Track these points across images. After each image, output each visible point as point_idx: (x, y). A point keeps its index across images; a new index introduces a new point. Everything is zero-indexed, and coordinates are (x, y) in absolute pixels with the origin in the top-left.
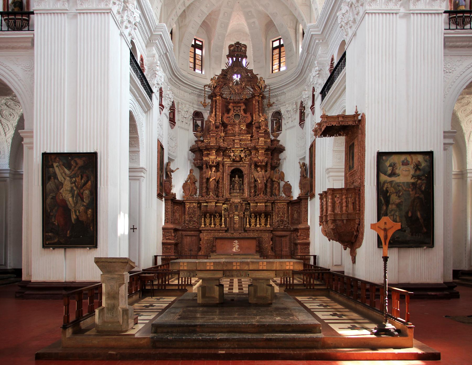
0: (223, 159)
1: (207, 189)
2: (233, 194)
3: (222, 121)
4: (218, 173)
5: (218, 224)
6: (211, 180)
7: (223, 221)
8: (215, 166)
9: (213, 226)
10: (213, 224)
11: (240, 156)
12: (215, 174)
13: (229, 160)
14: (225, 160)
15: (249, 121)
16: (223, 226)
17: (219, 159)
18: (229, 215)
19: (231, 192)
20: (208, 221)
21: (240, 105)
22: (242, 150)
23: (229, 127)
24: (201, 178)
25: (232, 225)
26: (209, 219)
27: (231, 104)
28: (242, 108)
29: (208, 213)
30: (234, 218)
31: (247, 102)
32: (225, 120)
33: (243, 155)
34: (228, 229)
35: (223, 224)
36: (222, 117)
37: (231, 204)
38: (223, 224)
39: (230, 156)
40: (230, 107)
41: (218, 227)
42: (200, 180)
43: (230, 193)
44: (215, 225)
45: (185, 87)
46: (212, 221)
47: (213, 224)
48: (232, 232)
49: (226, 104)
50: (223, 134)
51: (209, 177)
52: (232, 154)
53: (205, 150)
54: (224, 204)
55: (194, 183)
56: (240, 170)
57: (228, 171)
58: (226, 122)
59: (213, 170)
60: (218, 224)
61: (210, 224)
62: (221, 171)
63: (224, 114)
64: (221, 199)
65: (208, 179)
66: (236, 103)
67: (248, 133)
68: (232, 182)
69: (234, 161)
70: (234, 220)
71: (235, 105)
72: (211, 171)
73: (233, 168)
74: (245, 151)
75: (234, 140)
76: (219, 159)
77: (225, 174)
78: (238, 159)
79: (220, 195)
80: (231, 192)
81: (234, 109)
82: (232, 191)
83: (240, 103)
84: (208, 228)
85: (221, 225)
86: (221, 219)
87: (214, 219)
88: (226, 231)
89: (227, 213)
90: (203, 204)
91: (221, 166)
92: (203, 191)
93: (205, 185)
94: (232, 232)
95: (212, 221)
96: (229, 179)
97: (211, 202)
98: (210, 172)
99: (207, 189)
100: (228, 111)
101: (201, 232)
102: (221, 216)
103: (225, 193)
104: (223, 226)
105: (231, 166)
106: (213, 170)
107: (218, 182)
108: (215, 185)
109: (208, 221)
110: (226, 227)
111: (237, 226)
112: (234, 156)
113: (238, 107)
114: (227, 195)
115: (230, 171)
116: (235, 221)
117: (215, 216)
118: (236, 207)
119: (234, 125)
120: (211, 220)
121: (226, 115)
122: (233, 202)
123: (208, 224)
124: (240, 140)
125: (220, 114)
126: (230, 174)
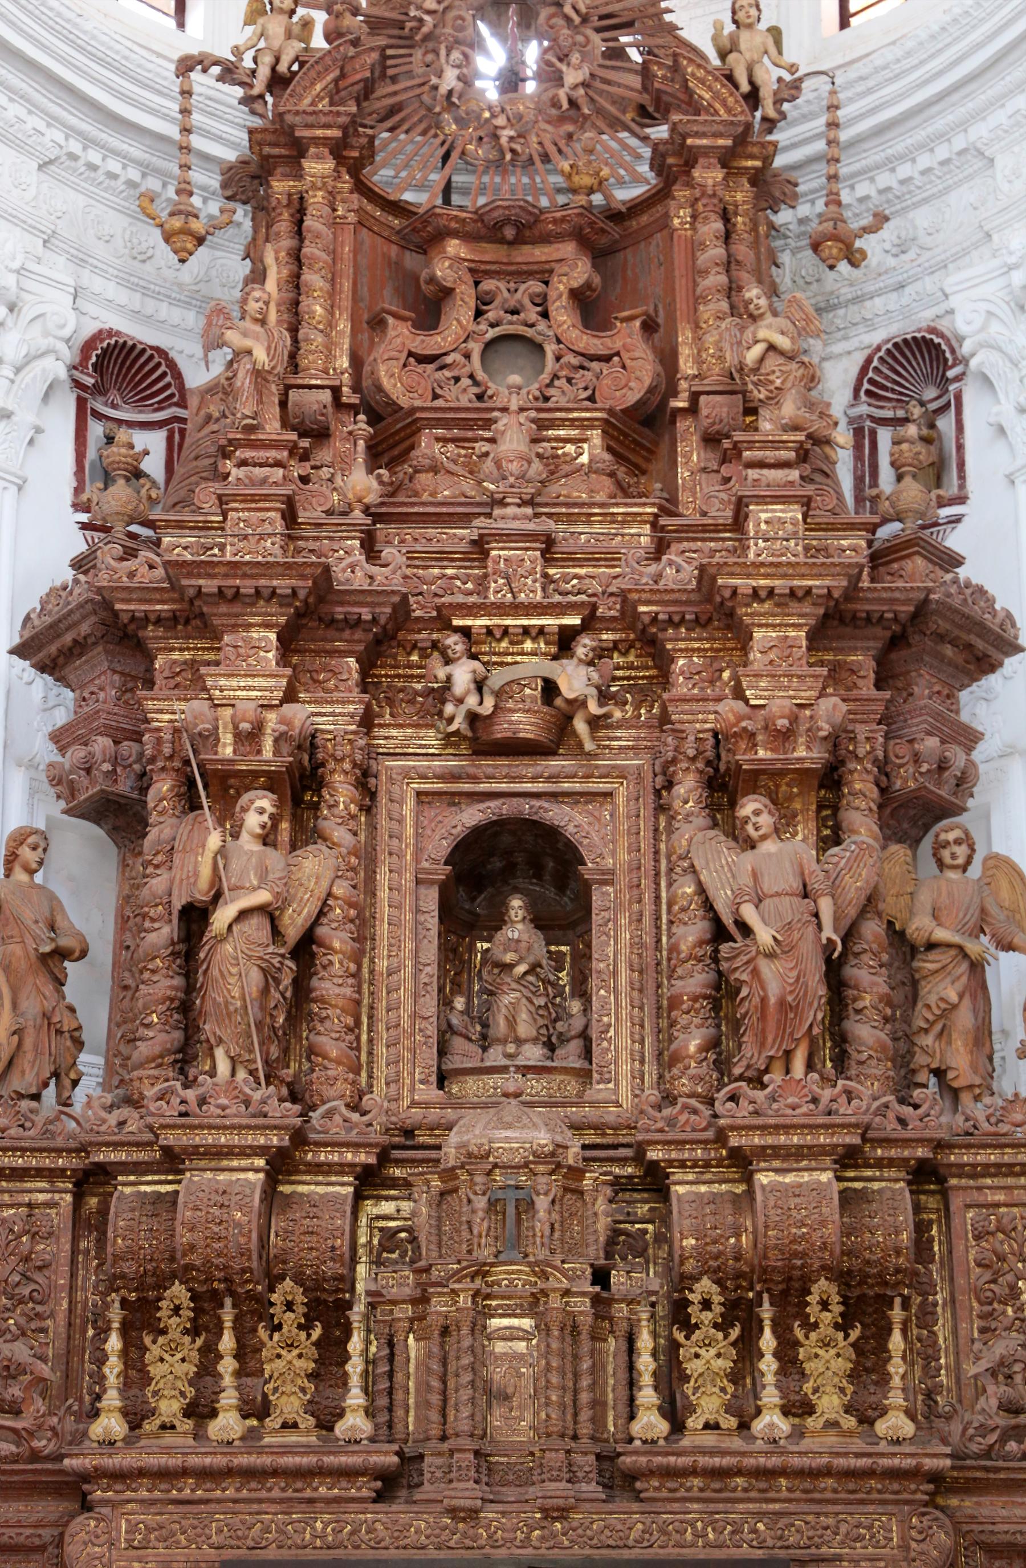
0: (367, 722)
1: (186, 1010)
2: (471, 1087)
3: (356, 388)
4: (315, 867)
5: (290, 1404)
6: (222, 917)
7: (355, 1367)
8: (272, 782)
9: (228, 1423)
10: (229, 1398)
11: (550, 689)
12: (275, 859)
13: (431, 739)
14: (392, 735)
15: (632, 382)
16: (354, 1422)
17: (324, 723)
18: (422, 1300)
19: (454, 1062)
20: (171, 1366)
21: (539, 253)
22: (564, 643)
23: (428, 446)
24: (131, 918)
25: (461, 1419)
26: (191, 1347)
27: (454, 247)
28: (560, 286)
29: (184, 1274)
30: (478, 1328)
31: (610, 235)
32: (395, 383)
33: (574, 679)
34: (410, 1461)
35: (355, 1398)
36: (357, 361)
37: (449, 1174)
38: (355, 1398)
39: (443, 692)
40: (442, 270)
41: (291, 1442)
42: (121, 946)
43: (442, 1079)
44: (257, 1409)
45: (34, 108)
46: (227, 1366)
47: (229, 1398)
48: (465, 1492)
49: (411, 260)
50: (362, 483)
51: (201, 893)
52: (462, 675)
53: (171, 622)
54: (369, 1181)
55: (55, 960)
56: (551, 833)
57: (418, 839)
58: (404, 402)
59: (253, 821)
60: (290, 1404)
61: (200, 1411)
62: (340, 834)
63: (377, 324)
64: (336, 1130)
65: (195, 918)
66: (510, 230)
67: (624, 490)
68: (455, 965)
69: (481, 740)
70: (480, 1358)
71: (490, 253)
72: (235, 836)
73: (472, 816)
74: (601, 653)
75: (480, 548)
76: (331, 714)
77: (383, 877)
78: (523, 722)
79: (333, 1087)
80: (454, 1062)
81: (483, 303)
82: (464, 1053)
83: (546, 239)
84: (176, 1448)
85: (326, 1419)
86: (331, 1354)
87: (247, 1353)
88: (390, 1485)
89: (400, 1283)
90: (128, 1188)
91: (341, 792)
92: (144, 1049)
93: (164, 984)
94: (465, 1492)
95: (227, 1366)
96: (433, 922)
97: (218, 1153)
98: (214, 840)
99: (186, 1010)
100: (429, 307)
101: (86, 1507)
102: (328, 1309)
103: (382, 1072)
104: (354, 1422)
105: (454, 799)
106: (253, 821)
107: (306, 949)
108: (270, 975)
109: (171, 1366)
110: (387, 1427)
111: (516, 1426)
112: (480, 685)
113: (522, 275)
114: (401, 1085)
115: (440, 846)
116: (498, 1374)
117: (256, 1311)
118: (512, 1210)
119: (474, 423)
120: (210, 1355)
121: (400, 334)
122: (475, 1158)
123: (170, 1408)
124: (548, 546)
125: (344, 325)
126: (443, 872)
